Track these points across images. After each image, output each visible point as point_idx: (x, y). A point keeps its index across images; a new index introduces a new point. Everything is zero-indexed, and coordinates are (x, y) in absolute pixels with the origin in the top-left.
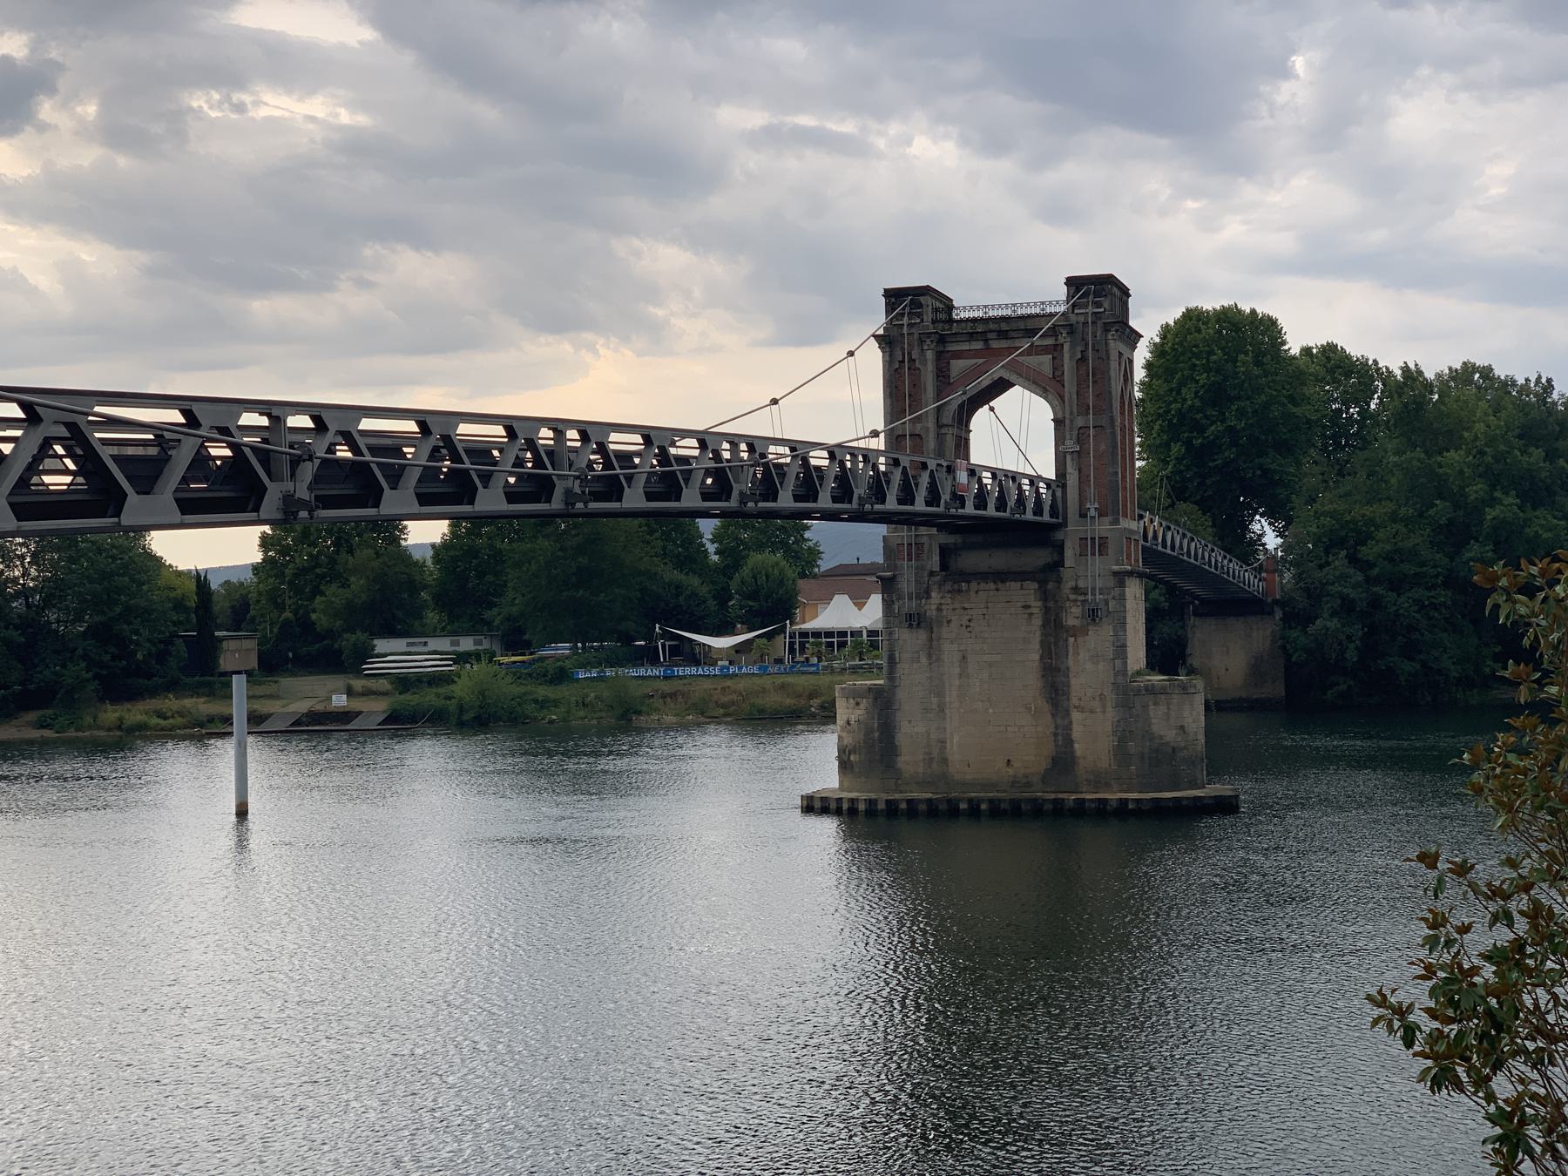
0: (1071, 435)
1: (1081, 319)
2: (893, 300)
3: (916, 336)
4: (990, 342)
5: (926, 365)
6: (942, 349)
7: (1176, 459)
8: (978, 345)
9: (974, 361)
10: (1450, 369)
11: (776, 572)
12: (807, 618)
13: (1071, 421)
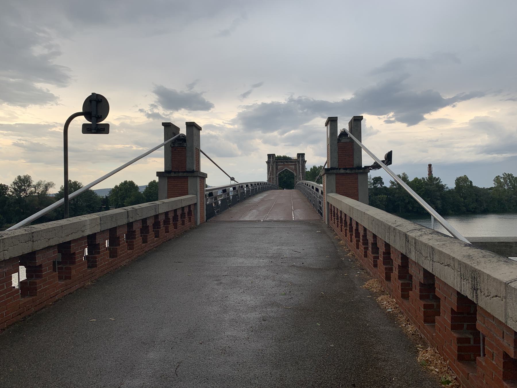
8: (283, 164)
10: (318, 167)
13: (298, 176)
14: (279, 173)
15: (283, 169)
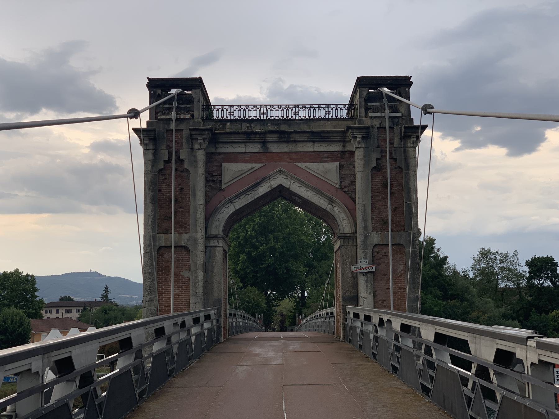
0: (365, 253)
1: (377, 123)
2: (159, 92)
3: (186, 133)
4: (269, 145)
5: (196, 167)
6: (213, 150)
7: (242, 262)
8: (255, 148)
9: (248, 166)
11: (18, 318)
12: (35, 341)
14: (228, 211)
15: (257, 185)
